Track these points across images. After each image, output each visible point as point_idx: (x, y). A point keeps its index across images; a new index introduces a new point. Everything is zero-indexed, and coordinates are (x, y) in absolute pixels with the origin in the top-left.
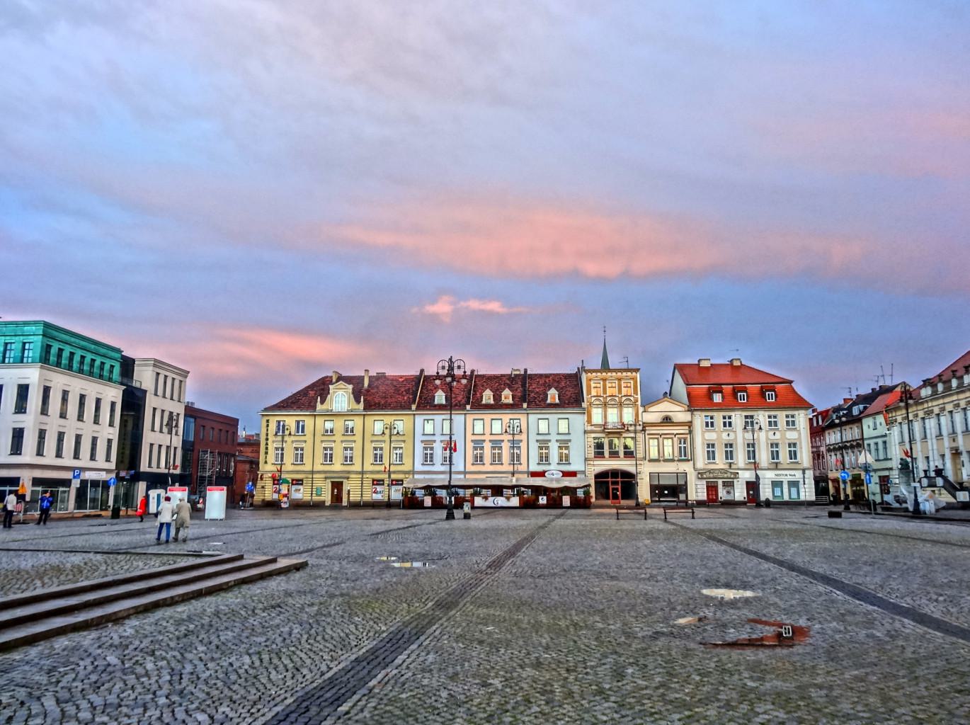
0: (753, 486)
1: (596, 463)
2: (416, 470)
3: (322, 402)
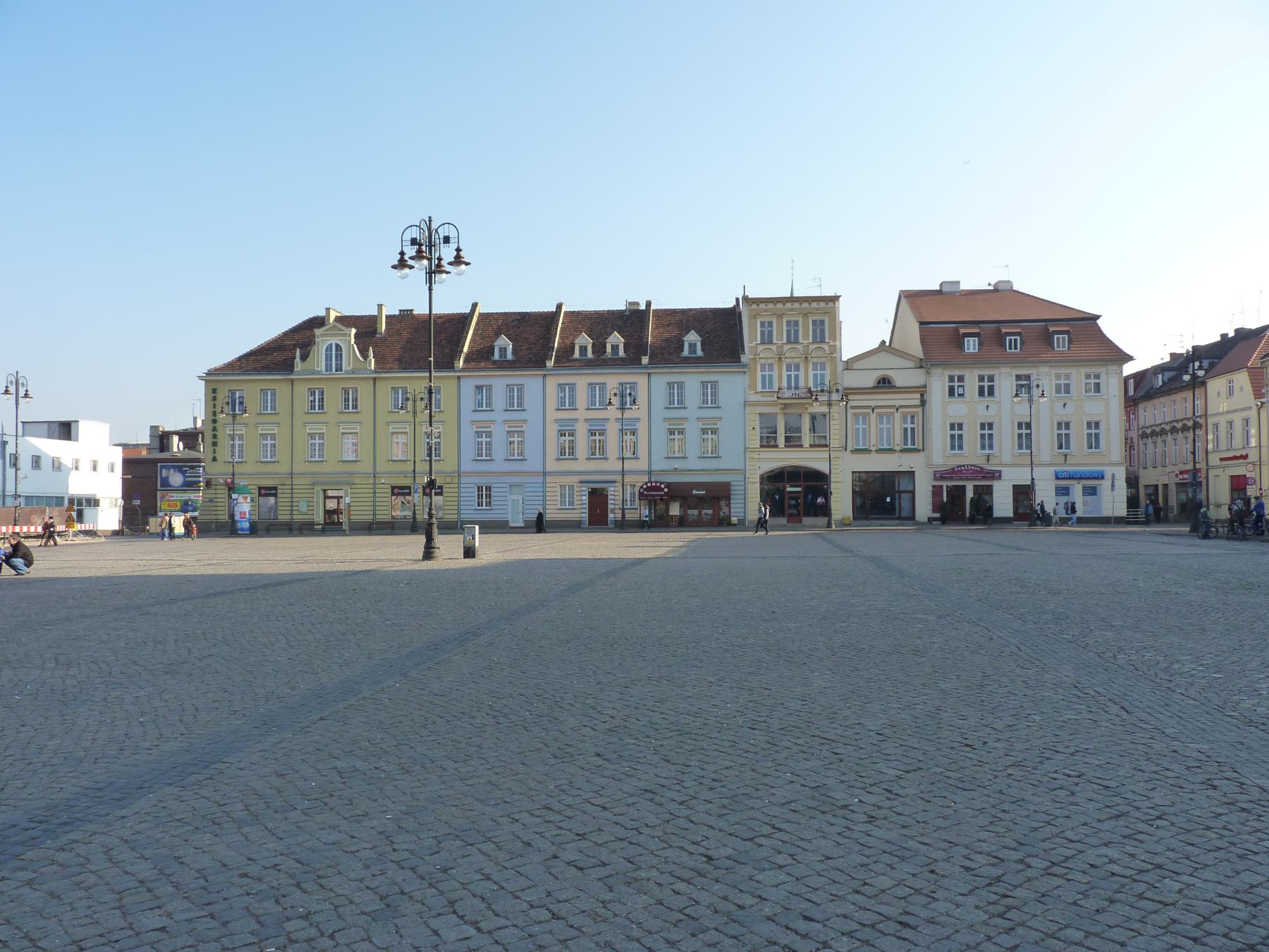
0: (1023, 493)
1: (763, 455)
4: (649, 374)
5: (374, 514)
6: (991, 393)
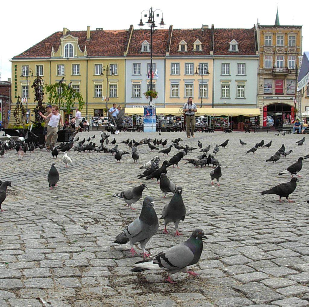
2: (127, 102)
3: (56, 51)
4: (214, 59)
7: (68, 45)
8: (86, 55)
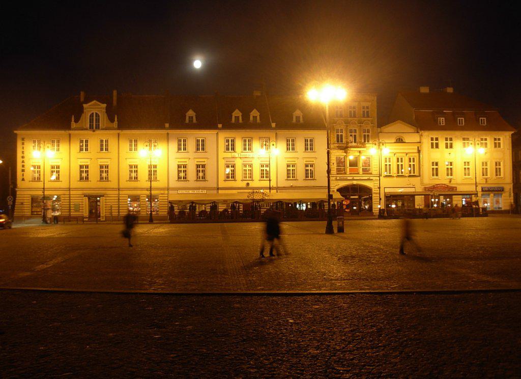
3: (76, 121)
5: (119, 212)
6: (451, 147)
7: (93, 113)
8: (117, 127)
